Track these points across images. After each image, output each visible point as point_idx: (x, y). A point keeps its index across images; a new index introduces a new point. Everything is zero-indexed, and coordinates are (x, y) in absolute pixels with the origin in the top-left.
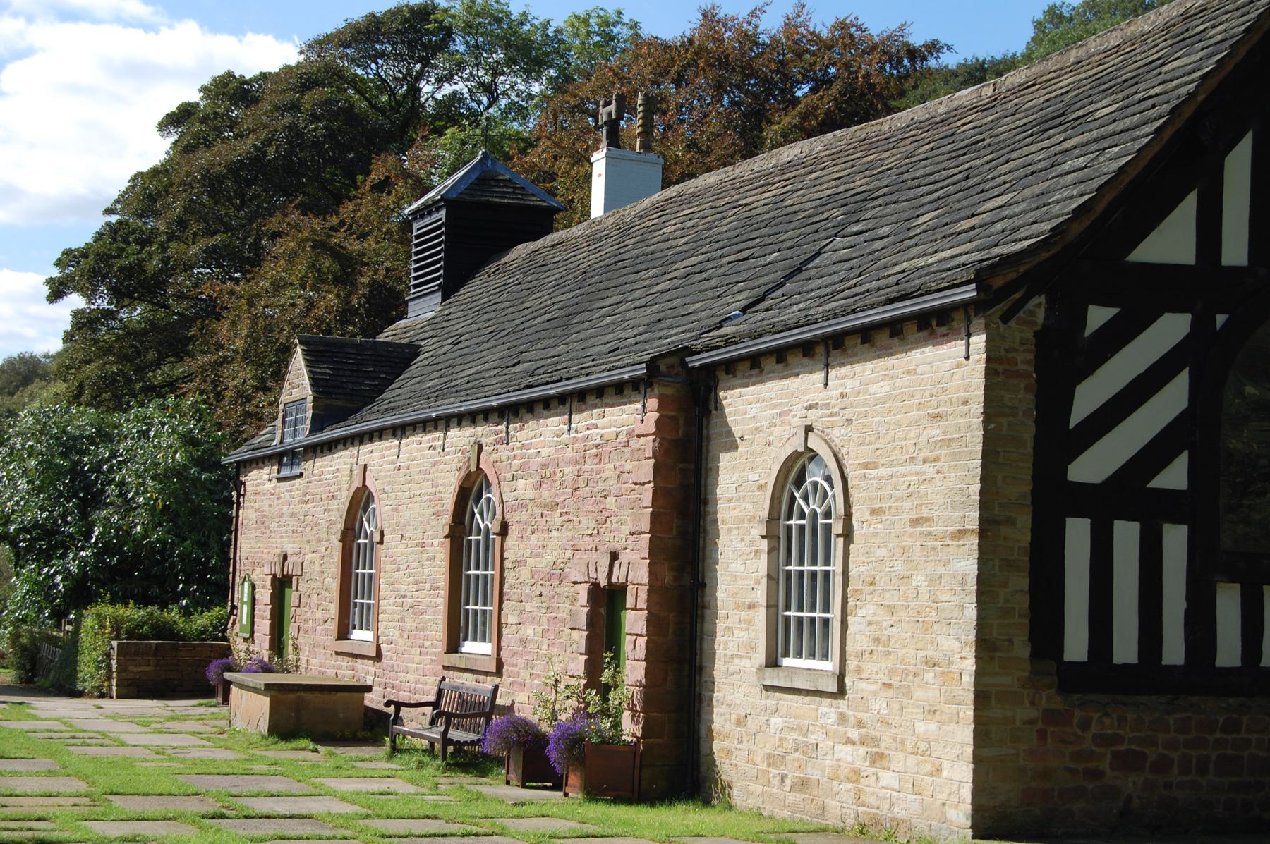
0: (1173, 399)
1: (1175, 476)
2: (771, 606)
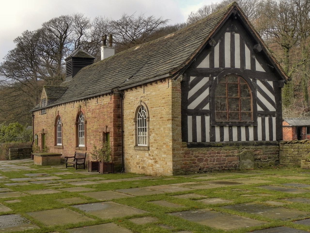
0: (206, 93)
1: (207, 107)
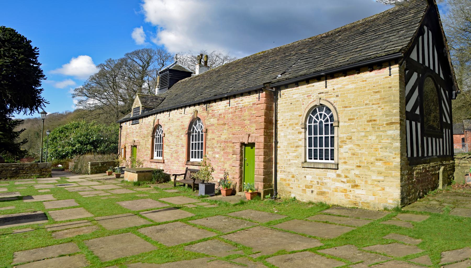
2: (305, 146)
